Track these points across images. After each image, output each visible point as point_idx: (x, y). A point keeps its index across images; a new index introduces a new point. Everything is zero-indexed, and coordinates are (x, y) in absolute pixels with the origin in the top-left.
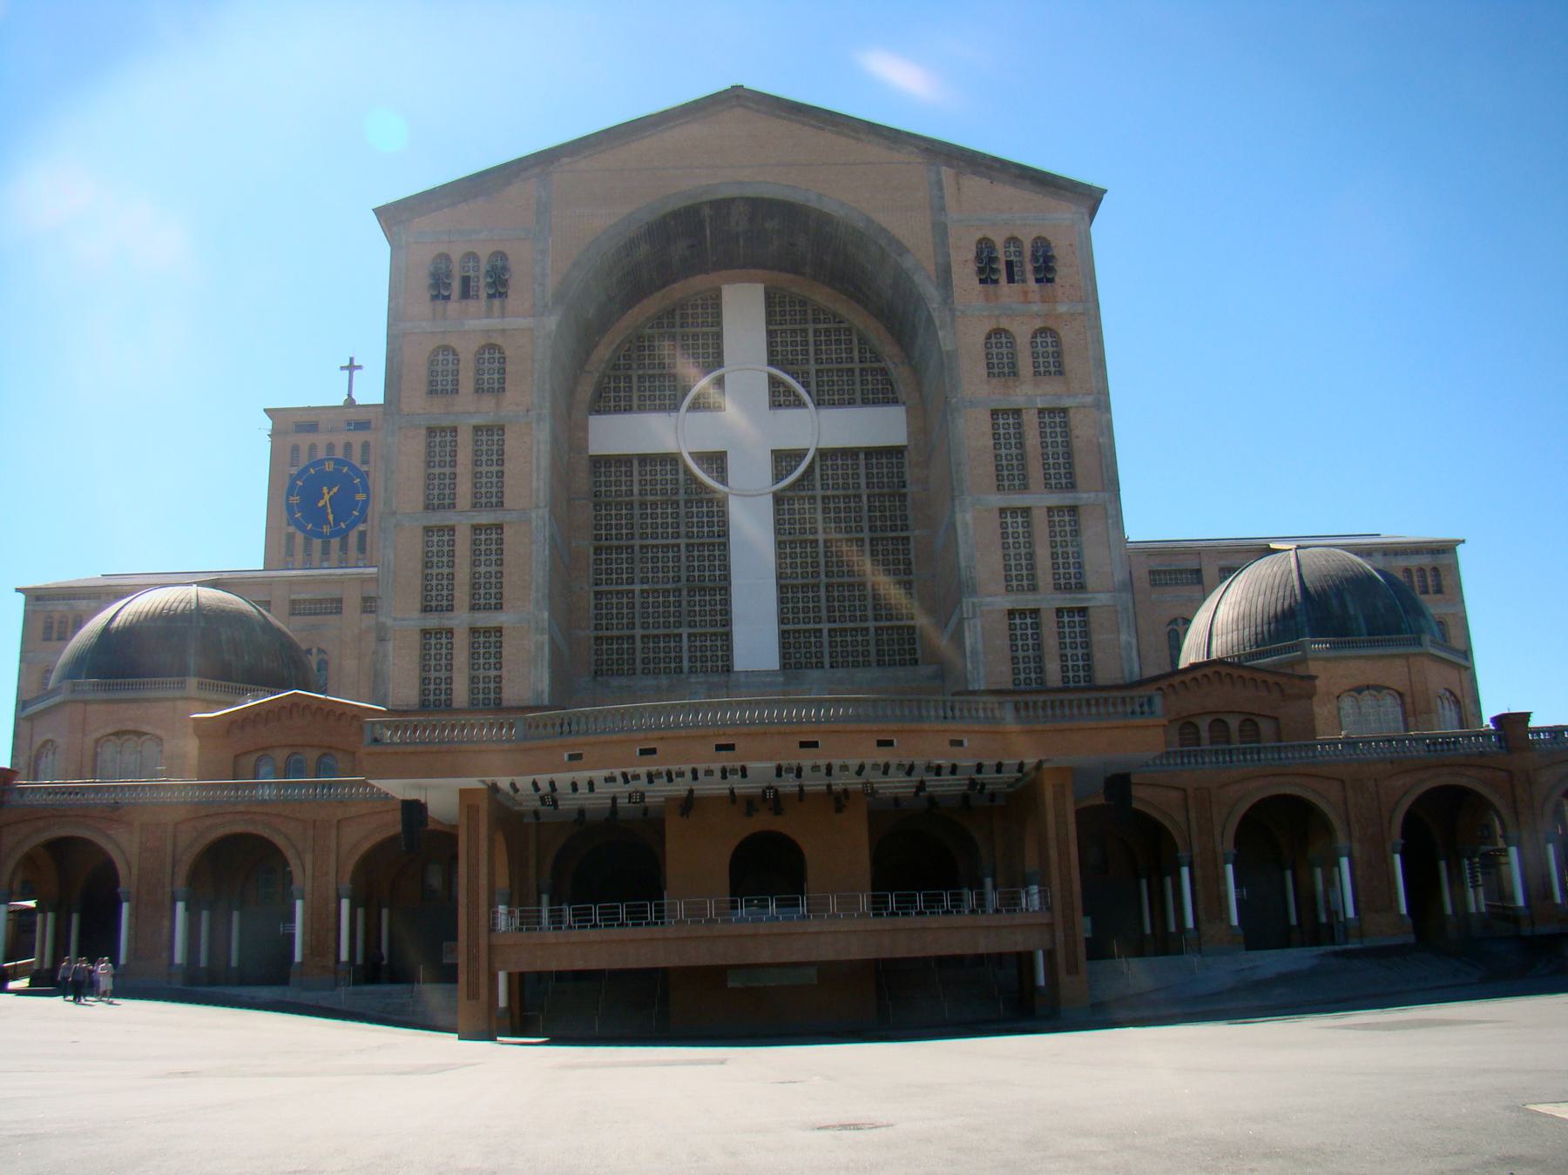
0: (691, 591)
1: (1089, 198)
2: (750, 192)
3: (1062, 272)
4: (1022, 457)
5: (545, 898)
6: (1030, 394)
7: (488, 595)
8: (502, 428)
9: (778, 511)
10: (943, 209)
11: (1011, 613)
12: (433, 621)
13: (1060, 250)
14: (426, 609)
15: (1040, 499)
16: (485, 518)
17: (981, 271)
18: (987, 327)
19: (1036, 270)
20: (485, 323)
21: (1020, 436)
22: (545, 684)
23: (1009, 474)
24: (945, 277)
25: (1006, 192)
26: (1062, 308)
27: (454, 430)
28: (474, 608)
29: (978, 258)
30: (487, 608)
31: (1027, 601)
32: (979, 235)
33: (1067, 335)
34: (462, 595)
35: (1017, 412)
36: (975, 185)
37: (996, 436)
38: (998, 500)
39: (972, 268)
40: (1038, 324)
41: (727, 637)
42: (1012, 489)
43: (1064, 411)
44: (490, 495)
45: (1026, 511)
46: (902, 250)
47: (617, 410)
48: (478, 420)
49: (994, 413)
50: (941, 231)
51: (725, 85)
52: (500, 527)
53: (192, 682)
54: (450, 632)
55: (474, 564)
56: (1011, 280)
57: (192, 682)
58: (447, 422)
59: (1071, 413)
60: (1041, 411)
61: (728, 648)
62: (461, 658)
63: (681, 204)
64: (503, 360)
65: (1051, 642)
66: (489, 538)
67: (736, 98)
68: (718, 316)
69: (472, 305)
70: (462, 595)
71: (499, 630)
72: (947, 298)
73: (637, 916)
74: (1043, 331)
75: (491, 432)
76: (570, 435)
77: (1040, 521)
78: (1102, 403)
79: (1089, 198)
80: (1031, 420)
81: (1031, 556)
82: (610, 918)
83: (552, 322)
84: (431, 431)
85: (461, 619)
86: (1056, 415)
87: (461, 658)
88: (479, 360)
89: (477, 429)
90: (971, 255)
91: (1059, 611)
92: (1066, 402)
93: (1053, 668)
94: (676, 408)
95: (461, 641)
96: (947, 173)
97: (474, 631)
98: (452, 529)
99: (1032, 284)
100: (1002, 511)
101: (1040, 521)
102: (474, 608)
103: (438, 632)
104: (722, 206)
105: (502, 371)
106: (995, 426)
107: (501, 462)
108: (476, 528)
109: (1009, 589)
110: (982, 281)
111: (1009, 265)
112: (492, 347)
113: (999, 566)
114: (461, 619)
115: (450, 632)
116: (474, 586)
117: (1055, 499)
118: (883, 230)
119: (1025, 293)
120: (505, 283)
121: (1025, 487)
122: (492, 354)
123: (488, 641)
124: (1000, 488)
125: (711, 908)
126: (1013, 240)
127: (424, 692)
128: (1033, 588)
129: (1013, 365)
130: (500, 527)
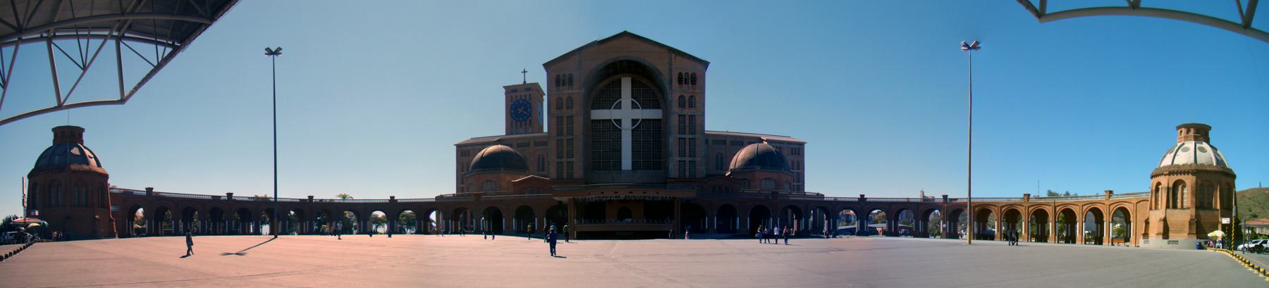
0: (613, 151)
1: (705, 64)
2: (627, 59)
3: (699, 82)
4: (685, 126)
5: (583, 218)
6: (687, 112)
7: (570, 155)
8: (572, 117)
9: (632, 134)
10: (671, 65)
11: (680, 161)
12: (559, 160)
13: (698, 77)
14: (558, 157)
15: (687, 136)
16: (570, 137)
17: (679, 81)
18: (680, 94)
19: (691, 81)
20: (570, 91)
21: (685, 121)
22: (582, 174)
23: (682, 131)
24: (671, 81)
25: (686, 61)
26: (697, 91)
27: (562, 117)
28: (568, 157)
29: (679, 78)
30: (570, 157)
31: (683, 159)
32: (679, 72)
33: (697, 98)
34: (565, 154)
35: (684, 116)
36: (679, 58)
37: (679, 121)
38: (678, 136)
39: (677, 80)
40: (691, 95)
41: (621, 162)
42: (682, 134)
43: (695, 116)
44: (570, 132)
45: (684, 139)
46: (662, 75)
47: (597, 109)
48: (567, 115)
49: (679, 116)
50: (671, 70)
51: (623, 31)
52: (572, 139)
53: (502, 169)
54: (563, 163)
55: (567, 147)
56: (686, 83)
57: (502, 169)
58: (561, 115)
59: (697, 117)
60: (690, 116)
61: (621, 164)
62: (565, 168)
63: (612, 61)
64: (572, 100)
65: (687, 168)
66: (570, 141)
67: (625, 34)
68: (620, 85)
69: (565, 87)
70: (565, 154)
71: (573, 162)
72: (671, 88)
73: (600, 222)
74: (692, 96)
75: (570, 118)
76: (587, 115)
77: (687, 141)
78: (703, 115)
79: (705, 64)
80: (687, 117)
81: (685, 149)
82: (595, 222)
83: (583, 91)
84: (558, 117)
85: (565, 160)
86: (692, 117)
87: (565, 168)
88: (567, 100)
89: (567, 117)
90: (677, 77)
91: (690, 161)
92: (695, 114)
93: (687, 174)
94: (610, 108)
95: (565, 164)
96: (673, 55)
97: (568, 162)
98: (562, 140)
99: (690, 85)
100: (679, 138)
101: (687, 141)
102: (568, 157)
103: (561, 163)
104: (621, 62)
105: (572, 103)
106: (679, 118)
107: (572, 124)
108: (568, 140)
109: (679, 156)
110: (679, 83)
111: (685, 79)
112: (570, 97)
113: (678, 151)
114: (565, 160)
115: (563, 163)
116: (567, 152)
117: (690, 136)
118: (657, 70)
119: (689, 87)
120: (572, 82)
121: (684, 133)
122: (570, 98)
123: (570, 164)
124: (679, 133)
125: (613, 221)
126: (687, 73)
127: (557, 175)
128: (685, 156)
129: (685, 104)
130: (572, 139)
